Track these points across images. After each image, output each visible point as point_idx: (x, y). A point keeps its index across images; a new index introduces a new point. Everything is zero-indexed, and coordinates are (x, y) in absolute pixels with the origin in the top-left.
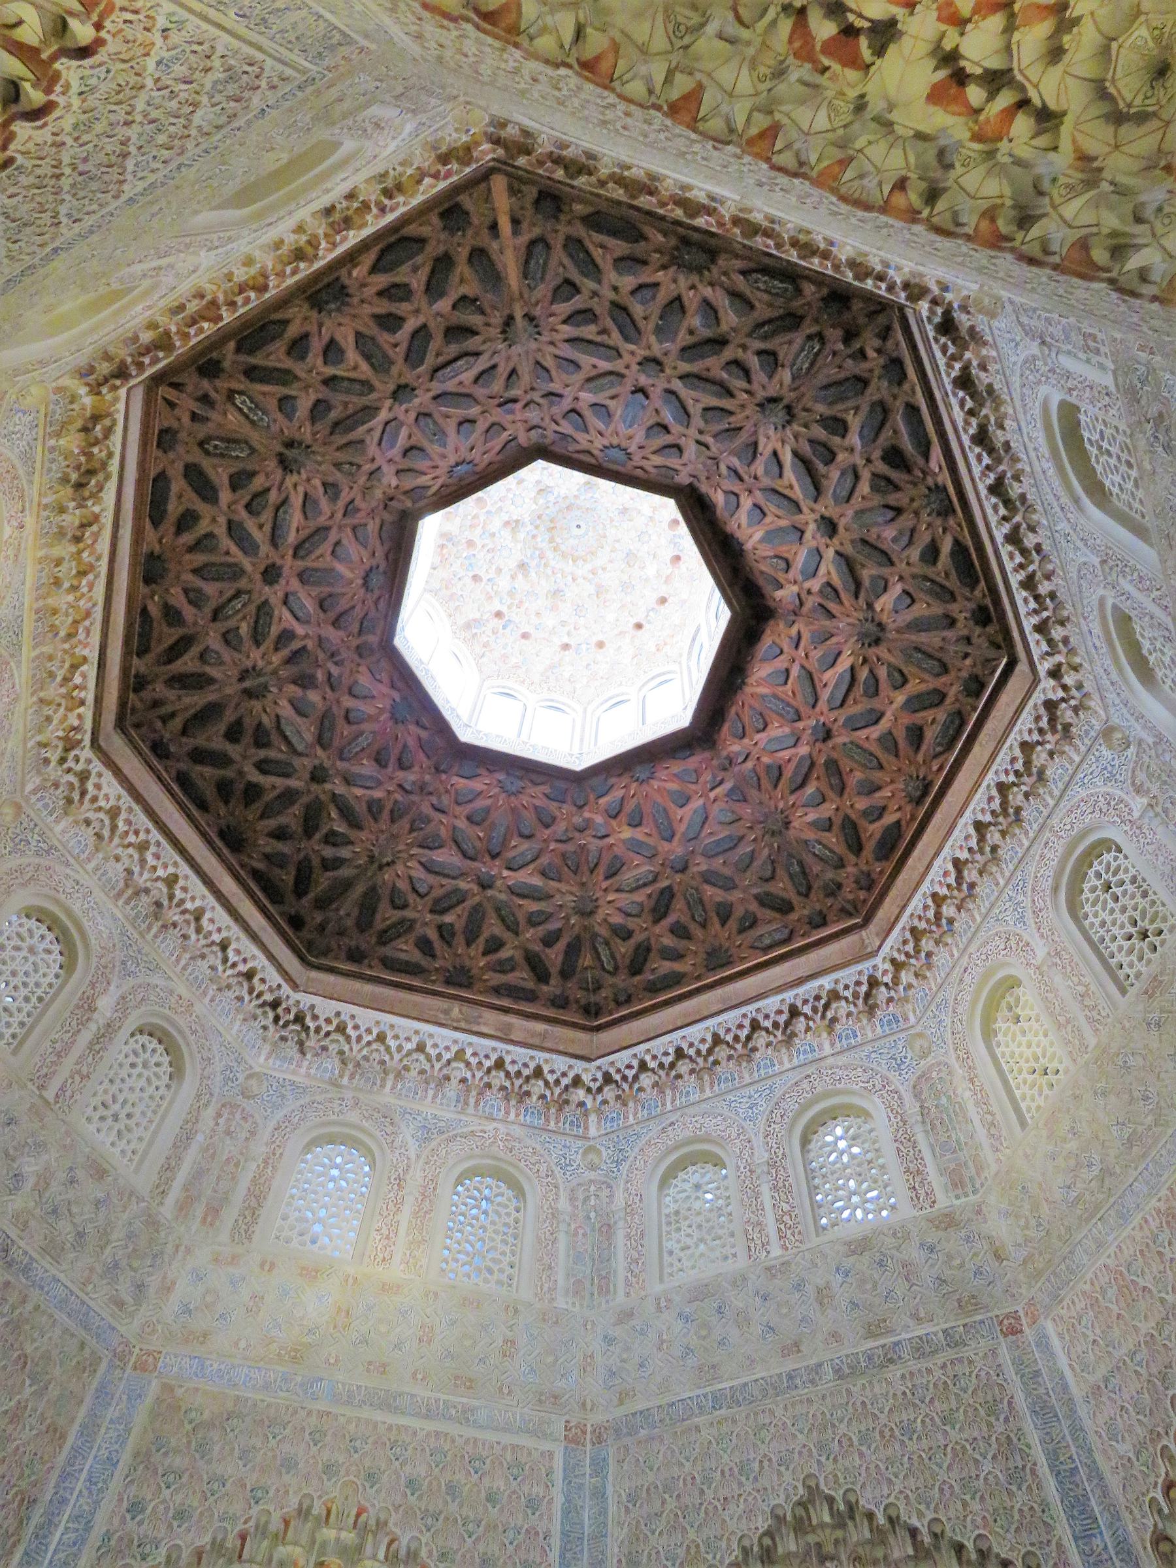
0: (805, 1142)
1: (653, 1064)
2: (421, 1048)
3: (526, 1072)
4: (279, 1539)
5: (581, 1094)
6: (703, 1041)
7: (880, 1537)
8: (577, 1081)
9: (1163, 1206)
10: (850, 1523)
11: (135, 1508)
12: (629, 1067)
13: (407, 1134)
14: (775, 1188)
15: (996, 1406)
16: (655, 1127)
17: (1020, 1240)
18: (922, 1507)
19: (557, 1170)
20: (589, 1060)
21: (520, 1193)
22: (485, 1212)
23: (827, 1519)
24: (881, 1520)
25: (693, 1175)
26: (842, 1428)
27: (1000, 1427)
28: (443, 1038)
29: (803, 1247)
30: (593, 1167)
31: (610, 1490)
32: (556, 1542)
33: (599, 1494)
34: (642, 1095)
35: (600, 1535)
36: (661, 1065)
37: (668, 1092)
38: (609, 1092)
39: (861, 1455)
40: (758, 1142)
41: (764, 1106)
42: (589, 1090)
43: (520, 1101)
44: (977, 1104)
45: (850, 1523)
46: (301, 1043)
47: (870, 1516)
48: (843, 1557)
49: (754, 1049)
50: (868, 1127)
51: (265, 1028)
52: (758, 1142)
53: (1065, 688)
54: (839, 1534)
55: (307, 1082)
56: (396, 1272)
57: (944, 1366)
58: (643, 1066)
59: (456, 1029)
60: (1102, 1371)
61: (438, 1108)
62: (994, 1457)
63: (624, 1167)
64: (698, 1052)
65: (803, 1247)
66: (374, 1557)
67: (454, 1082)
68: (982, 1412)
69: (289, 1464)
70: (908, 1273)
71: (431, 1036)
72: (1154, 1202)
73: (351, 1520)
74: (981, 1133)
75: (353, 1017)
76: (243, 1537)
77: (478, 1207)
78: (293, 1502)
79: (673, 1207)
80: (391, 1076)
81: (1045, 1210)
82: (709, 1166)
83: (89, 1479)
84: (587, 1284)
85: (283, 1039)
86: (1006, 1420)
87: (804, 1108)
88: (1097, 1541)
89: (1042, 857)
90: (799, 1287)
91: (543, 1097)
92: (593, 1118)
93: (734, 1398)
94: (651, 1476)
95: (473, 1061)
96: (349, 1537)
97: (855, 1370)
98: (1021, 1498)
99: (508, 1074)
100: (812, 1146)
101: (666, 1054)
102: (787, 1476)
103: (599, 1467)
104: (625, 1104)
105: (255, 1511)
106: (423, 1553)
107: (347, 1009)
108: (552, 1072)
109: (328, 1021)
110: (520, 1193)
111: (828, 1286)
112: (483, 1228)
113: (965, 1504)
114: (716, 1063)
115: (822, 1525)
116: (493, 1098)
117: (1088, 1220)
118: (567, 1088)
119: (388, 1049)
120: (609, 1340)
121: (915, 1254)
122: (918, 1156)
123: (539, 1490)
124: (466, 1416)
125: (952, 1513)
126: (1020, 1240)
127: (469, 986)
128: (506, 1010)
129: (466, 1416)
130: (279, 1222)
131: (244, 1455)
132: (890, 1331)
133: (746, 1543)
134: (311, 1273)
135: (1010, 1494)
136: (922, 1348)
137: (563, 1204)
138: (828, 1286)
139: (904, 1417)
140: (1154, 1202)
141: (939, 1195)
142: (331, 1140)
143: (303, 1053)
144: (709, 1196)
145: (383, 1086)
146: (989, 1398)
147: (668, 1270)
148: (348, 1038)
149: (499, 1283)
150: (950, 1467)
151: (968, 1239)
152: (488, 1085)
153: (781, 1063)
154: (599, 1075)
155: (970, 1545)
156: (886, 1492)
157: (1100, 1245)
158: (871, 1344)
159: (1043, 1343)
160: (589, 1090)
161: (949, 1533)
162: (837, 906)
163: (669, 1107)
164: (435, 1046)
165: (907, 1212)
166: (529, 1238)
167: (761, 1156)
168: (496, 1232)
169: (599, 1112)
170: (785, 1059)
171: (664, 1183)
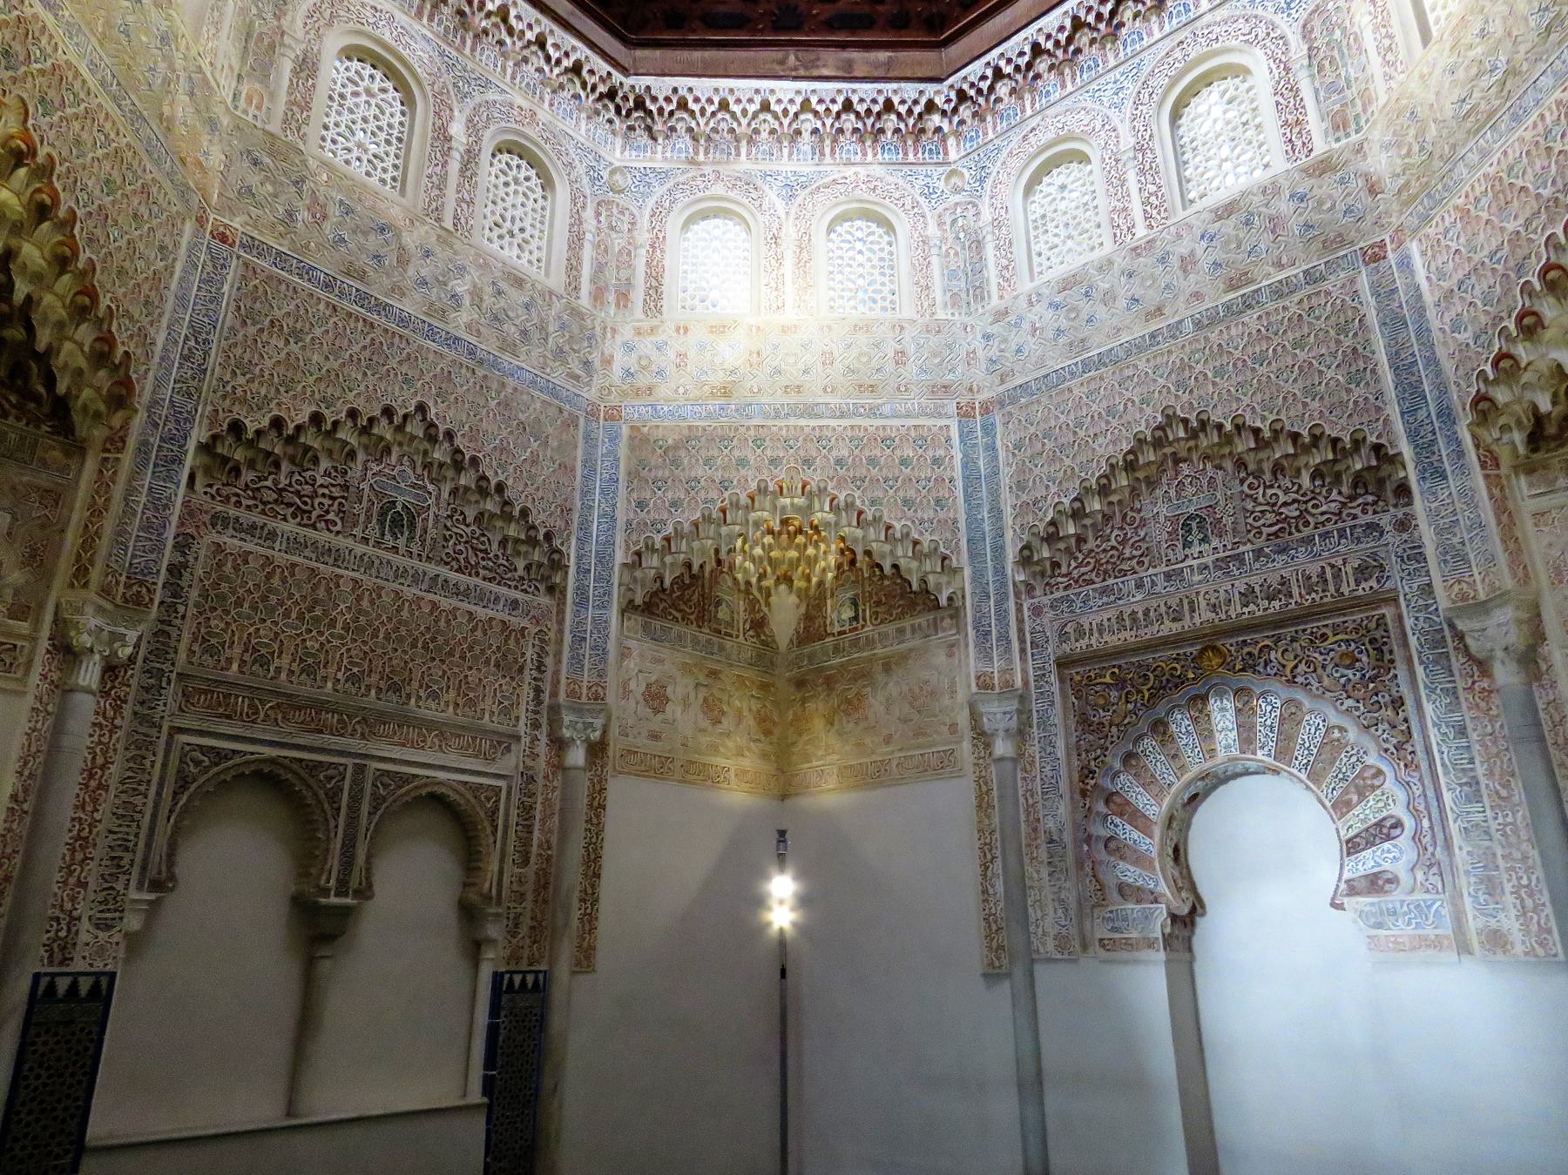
0: (1175, 116)
1: (1008, 69)
2: (765, 107)
3: (876, 109)
4: (750, 508)
5: (936, 119)
6: (1062, 29)
7: (1227, 439)
8: (931, 106)
10: (1202, 435)
11: (641, 505)
12: (984, 78)
13: (772, 196)
14: (1142, 172)
15: (1349, 322)
16: (1016, 138)
17: (1398, 170)
19: (922, 200)
20: (939, 80)
21: (889, 227)
22: (860, 252)
23: (1182, 434)
24: (1228, 427)
25: (1058, 177)
26: (1199, 367)
27: (1348, 342)
28: (785, 91)
29: (1169, 223)
30: (957, 190)
31: (999, 443)
32: (959, 483)
33: (991, 448)
34: (1000, 106)
35: (995, 473)
36: (1017, 68)
37: (1027, 96)
38: (965, 111)
39: (1214, 384)
40: (1124, 129)
41: (1131, 88)
42: (944, 113)
43: (875, 141)
44: (1376, 30)
45: (1202, 435)
46: (649, 129)
47: (1220, 427)
48: (1195, 459)
49: (1121, 25)
50: (1246, 85)
51: (610, 121)
54: (1192, 443)
55: (666, 166)
56: (790, 316)
58: (998, 74)
59: (796, 78)
60: (1460, 274)
61: (796, 163)
63: (989, 182)
64: (1057, 43)
65: (1169, 223)
66: (822, 510)
67: (806, 135)
68: (1332, 333)
69: (742, 462)
70: (1275, 225)
71: (772, 91)
73: (799, 490)
74: (1375, 61)
75: (690, 90)
76: (724, 511)
77: (853, 248)
78: (753, 486)
79: (1040, 211)
80: (744, 143)
81: (1433, 131)
82: (1075, 165)
83: (602, 492)
84: (964, 295)
85: (631, 128)
86: (1356, 334)
87: (1174, 81)
88: (1422, 414)
90: (1163, 260)
91: (897, 131)
92: (951, 141)
93: (1101, 361)
94: (1032, 430)
95: (821, 108)
96: (800, 501)
98: (1358, 392)
99: (857, 114)
100: (1183, 121)
101: (1022, 54)
102: (1149, 411)
103: (988, 430)
104: (983, 120)
105: (726, 494)
106: (858, 503)
107: (683, 83)
108: (903, 102)
109: (668, 100)
110: (889, 227)
111: (1192, 253)
112: (861, 265)
113: (1305, 405)
114: (1078, 51)
115: (1178, 440)
116: (848, 143)
117: (1478, 131)
118: (920, 115)
119: (733, 115)
120: (987, 337)
121: (1284, 206)
122: (1300, 106)
123: (941, 452)
124: (873, 412)
125: (1292, 414)
126: (1398, 170)
127: (798, 28)
128: (843, 46)
129: (873, 412)
130: (681, 295)
131: (708, 462)
132: (1252, 281)
133: (1113, 461)
134: (720, 329)
135: (1349, 391)
136: (1279, 291)
137: (932, 230)
138: (1192, 253)
139: (1257, 349)
142: (705, 215)
143: (655, 140)
144: (1075, 195)
145: (738, 154)
146: (1342, 320)
147: (1036, 270)
148: (692, 113)
149: (884, 309)
150: (1295, 380)
151: (1342, 181)
152: (841, 131)
153: (1150, 34)
154: (953, 95)
155: (1305, 433)
156: (1235, 406)
157: (1485, 154)
159: (1405, 264)
160: (944, 113)
161: (1287, 428)
163: (1029, 112)
164: (779, 101)
165: (1280, 165)
166: (904, 266)
167: (1127, 141)
168: (873, 267)
169: (957, 134)
170: (1155, 27)
171: (1029, 190)
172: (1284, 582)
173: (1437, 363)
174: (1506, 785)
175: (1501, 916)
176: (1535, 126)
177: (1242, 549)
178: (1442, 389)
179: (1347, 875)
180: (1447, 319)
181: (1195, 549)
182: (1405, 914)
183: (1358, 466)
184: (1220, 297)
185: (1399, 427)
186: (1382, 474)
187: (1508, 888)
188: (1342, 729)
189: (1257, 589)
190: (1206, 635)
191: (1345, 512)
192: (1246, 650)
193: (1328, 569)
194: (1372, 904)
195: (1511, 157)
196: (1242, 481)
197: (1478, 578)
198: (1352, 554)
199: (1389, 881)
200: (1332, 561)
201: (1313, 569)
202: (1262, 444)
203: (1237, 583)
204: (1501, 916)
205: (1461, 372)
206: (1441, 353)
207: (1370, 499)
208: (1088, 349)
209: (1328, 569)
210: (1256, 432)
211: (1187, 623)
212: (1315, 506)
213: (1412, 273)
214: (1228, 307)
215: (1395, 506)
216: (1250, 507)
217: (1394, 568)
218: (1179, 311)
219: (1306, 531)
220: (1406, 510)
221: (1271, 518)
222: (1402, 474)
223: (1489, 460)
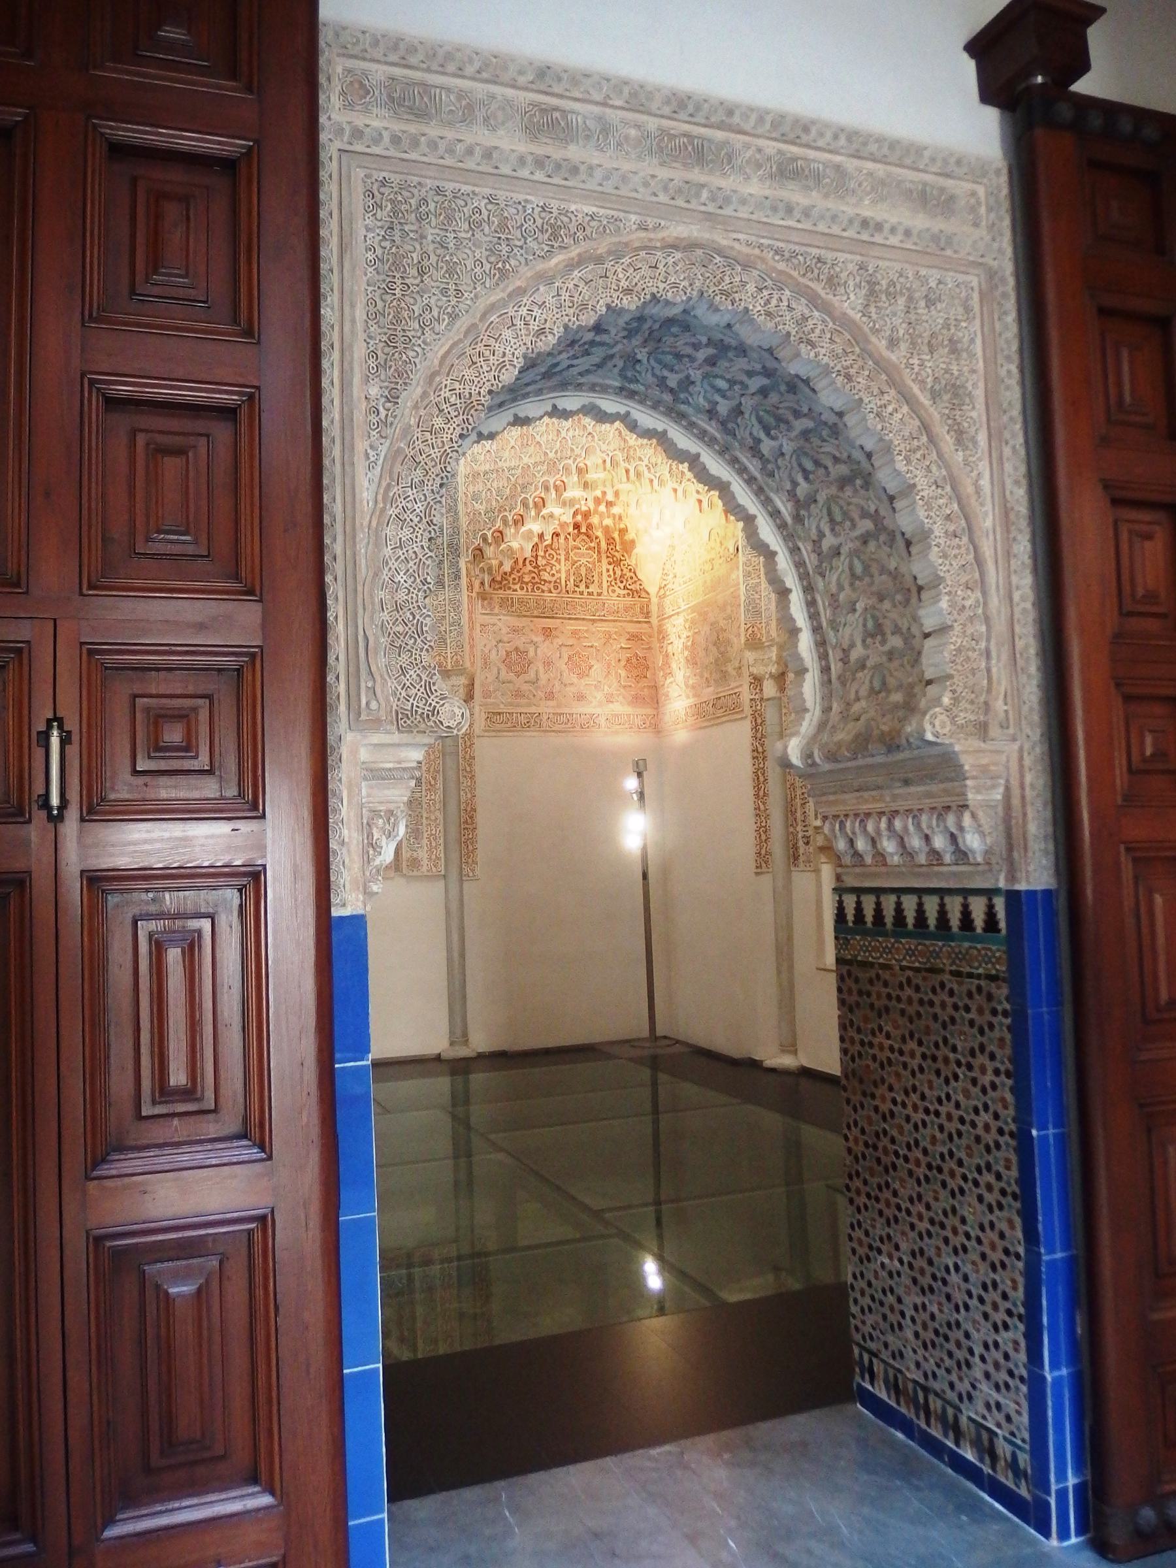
173: (456, 513)
174: (435, 779)
175: (419, 851)
180: (471, 489)
187: (425, 835)
204: (419, 851)
206: (460, 507)
223: (470, 587)
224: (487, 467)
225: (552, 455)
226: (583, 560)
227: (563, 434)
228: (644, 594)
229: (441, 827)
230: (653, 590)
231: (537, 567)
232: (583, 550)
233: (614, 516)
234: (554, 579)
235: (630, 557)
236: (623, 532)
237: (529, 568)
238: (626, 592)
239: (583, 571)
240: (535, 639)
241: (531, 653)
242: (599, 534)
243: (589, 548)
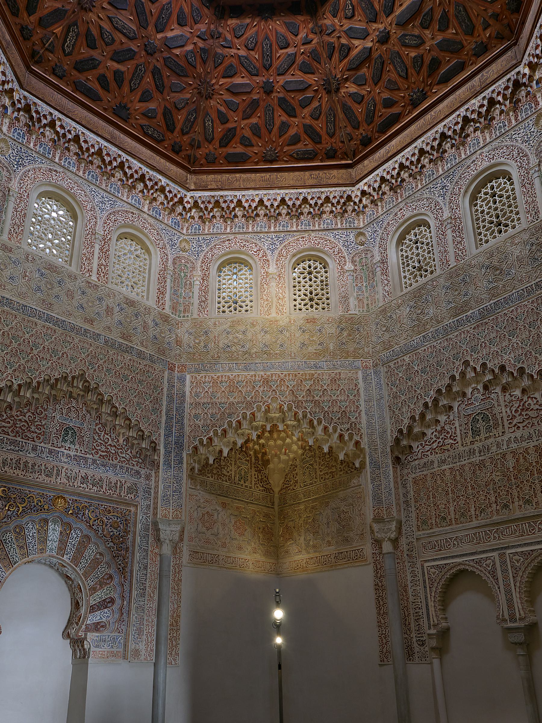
9: (265, 376)
18: (121, 403)
40: (100, 223)
52: (100, 223)
53: (361, 201)
54: (82, 393)
57: (146, 365)
62: (151, 401)
68: (152, 387)
72: (262, 373)
86: (159, 394)
89: (298, 240)
97: (112, 346)
98: (153, 417)
136: (140, 354)
140: (262, 373)
141: (167, 307)
150: (135, 396)
156: (110, 391)
158: (121, 341)
159: (182, 380)
162: (189, 152)
172: (101, 480)
173: (182, 424)
176: (252, 376)
177: (88, 456)
178: (181, 435)
179: (89, 622)
181: (67, 445)
182: (108, 641)
183: (144, 446)
184: (115, 336)
185: (162, 438)
186: (148, 454)
188: (101, 554)
189: (89, 478)
190: (60, 490)
191: (131, 461)
192: (76, 505)
193: (119, 482)
194: (98, 637)
195: (240, 379)
196: (97, 424)
197: (171, 510)
198: (129, 480)
199: (102, 626)
200: (121, 480)
201: (113, 480)
202: (115, 415)
203: (81, 471)
205: (192, 434)
206: (186, 421)
207: (140, 461)
208: (52, 311)
209: (119, 482)
210: (114, 406)
211: (53, 479)
212: (121, 453)
213: (184, 385)
214: (120, 345)
215: (147, 468)
216: (96, 438)
217: (141, 493)
218: (97, 329)
219: (115, 462)
220: (150, 472)
221: (104, 449)
222: (156, 458)
224: (206, 401)
225: (249, 399)
226: (243, 467)
227: (257, 388)
228: (271, 492)
229: (155, 628)
230: (277, 490)
231: (220, 465)
232: (243, 461)
233: (260, 444)
234: (229, 474)
235: (265, 469)
236: (265, 454)
237: (216, 465)
238: (263, 488)
239: (243, 474)
240: (218, 508)
241: (215, 517)
242: (251, 453)
243: (246, 460)
